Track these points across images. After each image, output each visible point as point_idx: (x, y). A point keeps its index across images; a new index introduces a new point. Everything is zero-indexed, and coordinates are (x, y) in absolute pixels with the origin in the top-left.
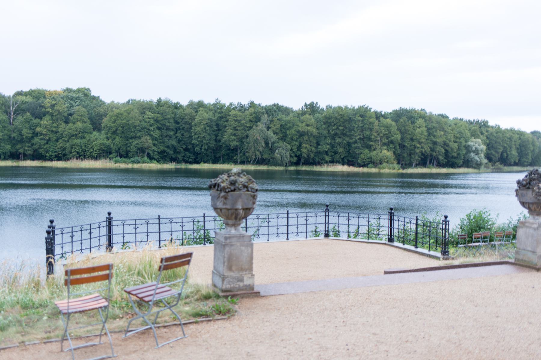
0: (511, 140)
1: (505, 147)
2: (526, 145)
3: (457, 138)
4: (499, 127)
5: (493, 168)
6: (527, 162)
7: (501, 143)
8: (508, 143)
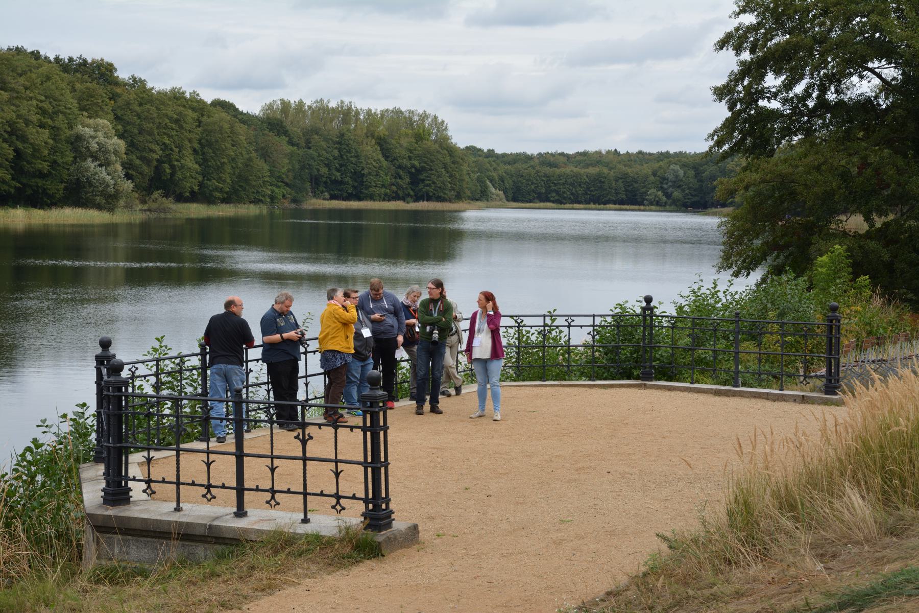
0: (181, 127)
1: (165, 147)
2: (217, 141)
3: (44, 112)
4: (142, 82)
5: (146, 207)
6: (221, 191)
7: (156, 132)
8: (174, 133)
